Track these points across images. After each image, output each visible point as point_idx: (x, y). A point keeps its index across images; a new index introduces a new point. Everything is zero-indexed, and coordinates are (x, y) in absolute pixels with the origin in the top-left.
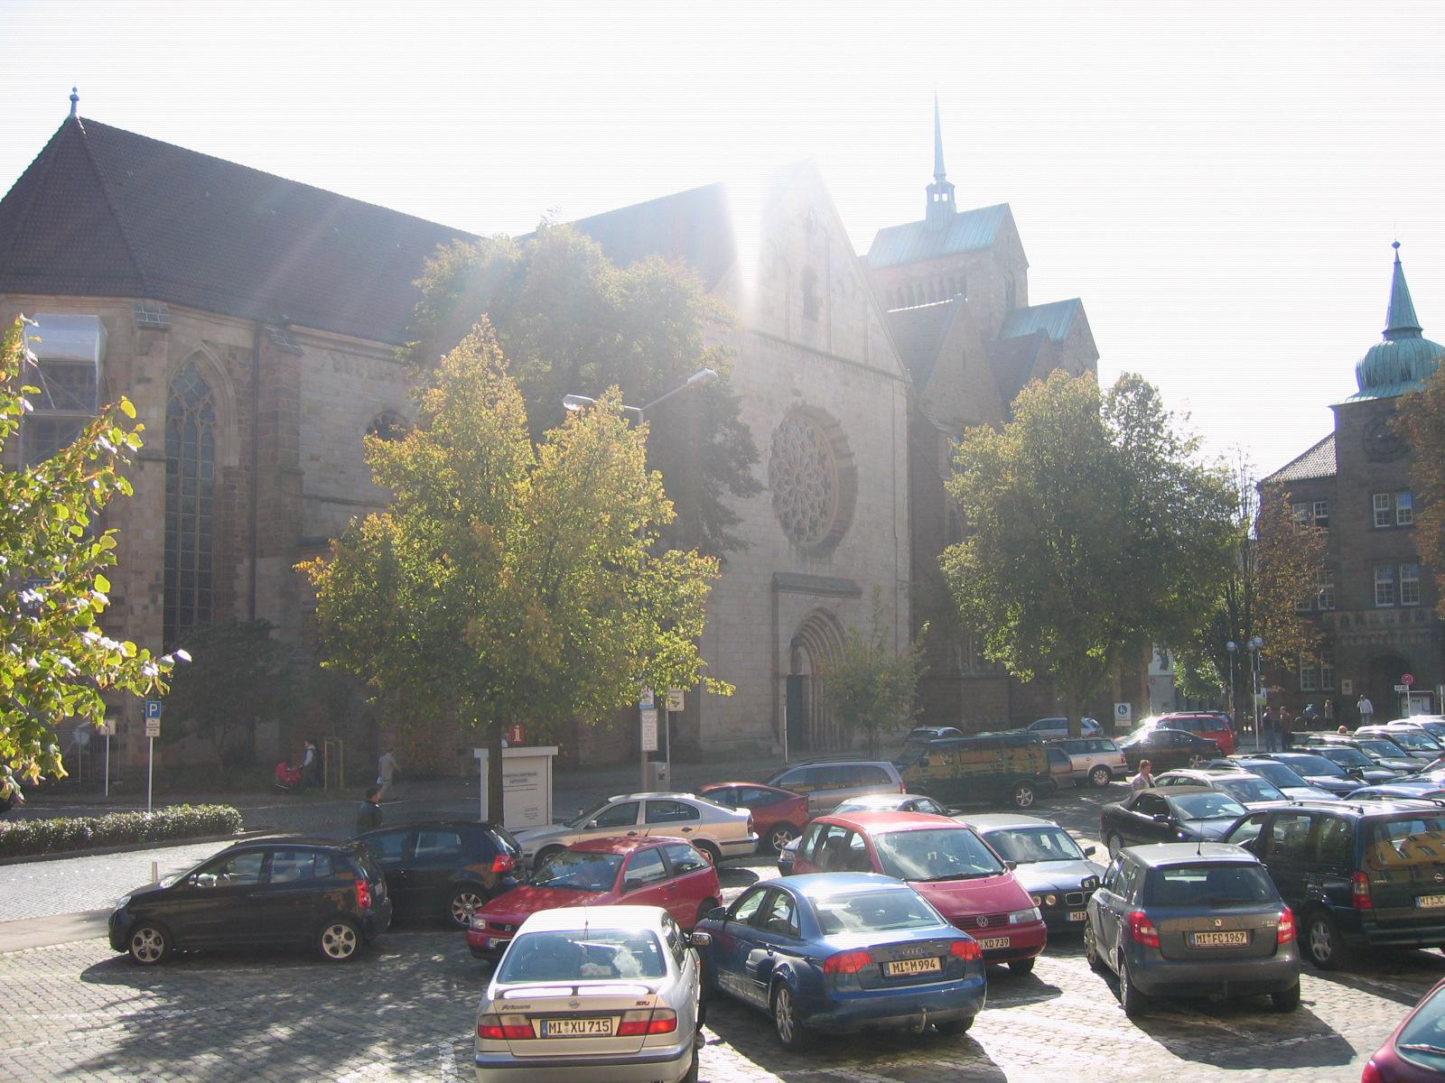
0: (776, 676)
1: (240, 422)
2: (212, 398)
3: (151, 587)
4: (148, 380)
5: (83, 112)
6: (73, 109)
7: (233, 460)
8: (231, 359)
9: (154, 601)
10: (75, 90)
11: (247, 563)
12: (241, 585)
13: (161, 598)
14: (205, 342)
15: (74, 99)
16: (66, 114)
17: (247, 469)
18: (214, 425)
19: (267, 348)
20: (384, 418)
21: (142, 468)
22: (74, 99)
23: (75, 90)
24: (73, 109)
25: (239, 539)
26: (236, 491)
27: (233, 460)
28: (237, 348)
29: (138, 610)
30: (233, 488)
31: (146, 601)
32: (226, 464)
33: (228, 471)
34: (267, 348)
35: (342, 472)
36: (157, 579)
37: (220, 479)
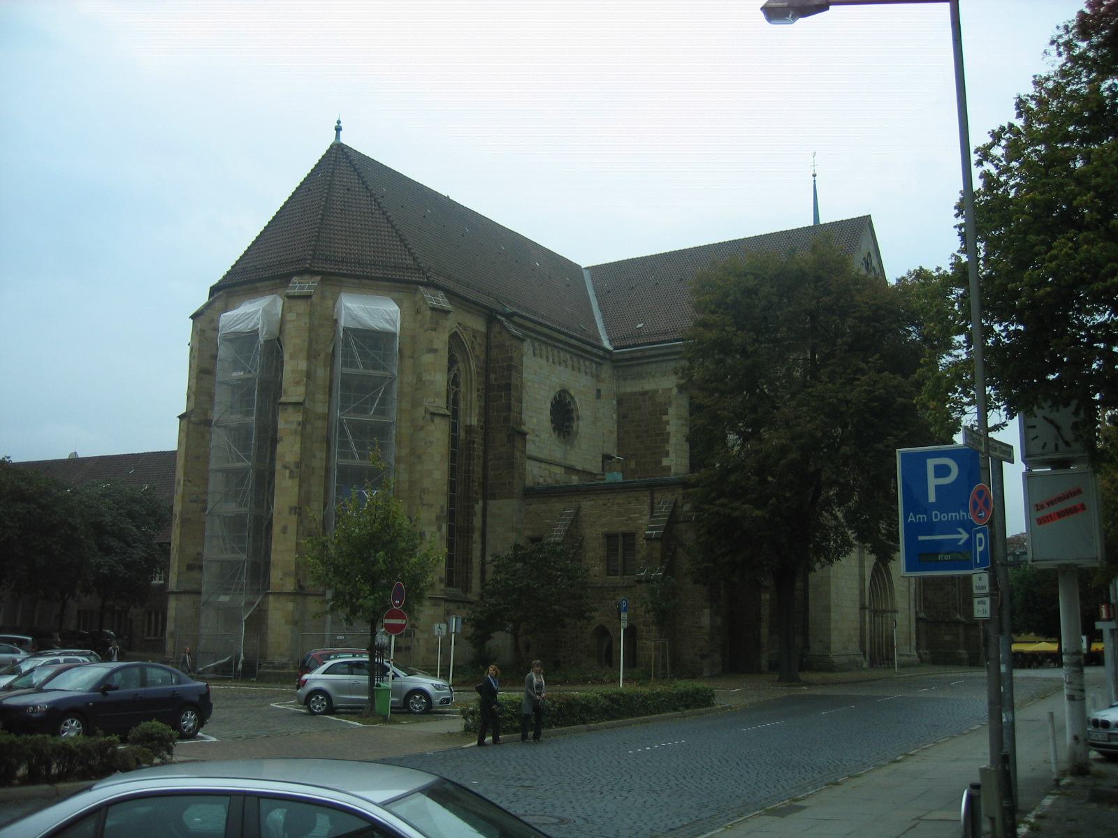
0: (863, 608)
1: (478, 390)
2: (458, 370)
3: (438, 518)
4: (435, 351)
5: (344, 140)
6: (338, 136)
7: (474, 421)
8: (473, 339)
9: (439, 529)
10: (339, 122)
11: (481, 503)
12: (477, 522)
13: (444, 527)
14: (459, 324)
15: (338, 129)
16: (332, 139)
17: (482, 428)
18: (460, 391)
19: (500, 333)
20: (560, 395)
21: (433, 421)
22: (338, 129)
23: (339, 122)
24: (338, 136)
25: (476, 484)
26: (475, 445)
27: (474, 421)
28: (478, 331)
29: (428, 536)
30: (474, 443)
31: (434, 529)
32: (468, 423)
33: (469, 429)
34: (500, 333)
35: (537, 436)
36: (442, 512)
37: (462, 435)
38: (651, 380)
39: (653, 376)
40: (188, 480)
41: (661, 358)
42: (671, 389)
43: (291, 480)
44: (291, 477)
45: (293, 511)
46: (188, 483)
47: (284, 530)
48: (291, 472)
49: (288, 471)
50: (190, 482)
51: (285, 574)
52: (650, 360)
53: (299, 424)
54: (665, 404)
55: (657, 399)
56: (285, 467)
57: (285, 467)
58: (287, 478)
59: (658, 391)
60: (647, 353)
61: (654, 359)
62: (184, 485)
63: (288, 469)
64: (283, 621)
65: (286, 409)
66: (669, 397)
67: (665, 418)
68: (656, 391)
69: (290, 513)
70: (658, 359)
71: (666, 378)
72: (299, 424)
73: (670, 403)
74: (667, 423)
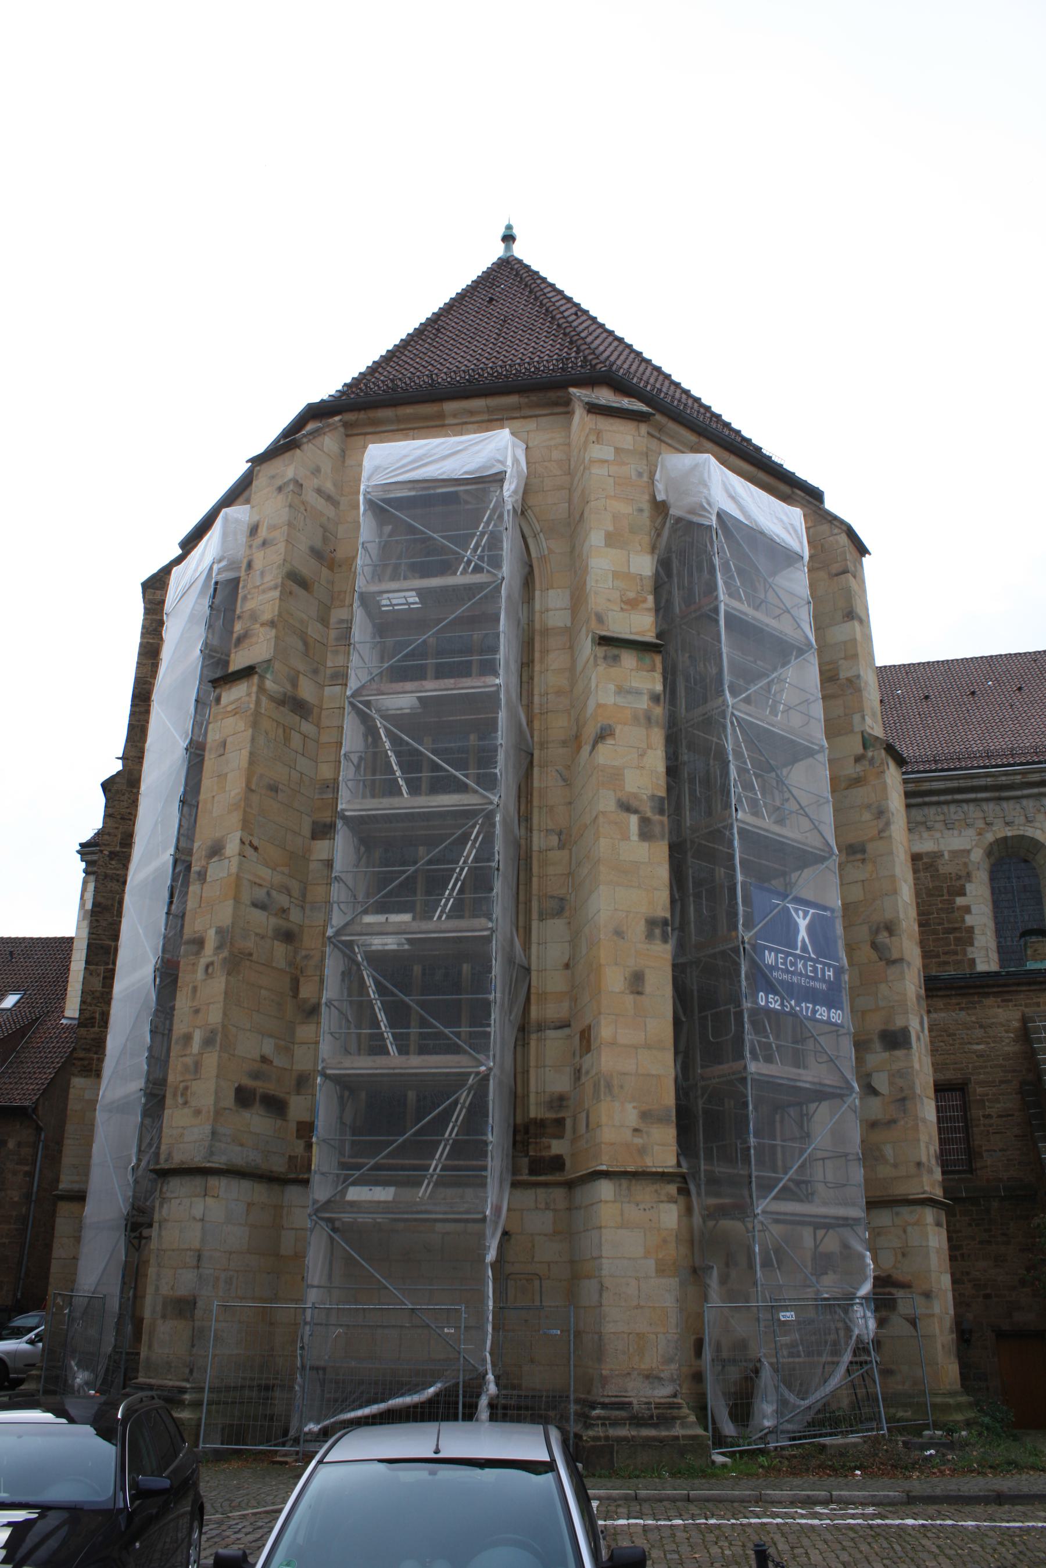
38: (925, 835)
39: (929, 829)
40: (251, 844)
41: (949, 797)
42: (969, 852)
43: (646, 845)
44: (645, 834)
45: (658, 932)
46: (249, 851)
47: (636, 982)
48: (644, 821)
49: (634, 819)
50: (256, 849)
51: (645, 1115)
52: (927, 799)
53: (655, 698)
54: (959, 878)
55: (940, 867)
56: (626, 807)
57: (626, 807)
58: (634, 837)
59: (943, 855)
60: (926, 786)
61: (935, 799)
62: (242, 855)
63: (636, 812)
64: (651, 1264)
65: (616, 658)
66: (965, 864)
67: (960, 901)
68: (937, 855)
69: (650, 936)
70: (942, 798)
71: (956, 832)
72: (655, 698)
73: (969, 875)
74: (967, 910)
